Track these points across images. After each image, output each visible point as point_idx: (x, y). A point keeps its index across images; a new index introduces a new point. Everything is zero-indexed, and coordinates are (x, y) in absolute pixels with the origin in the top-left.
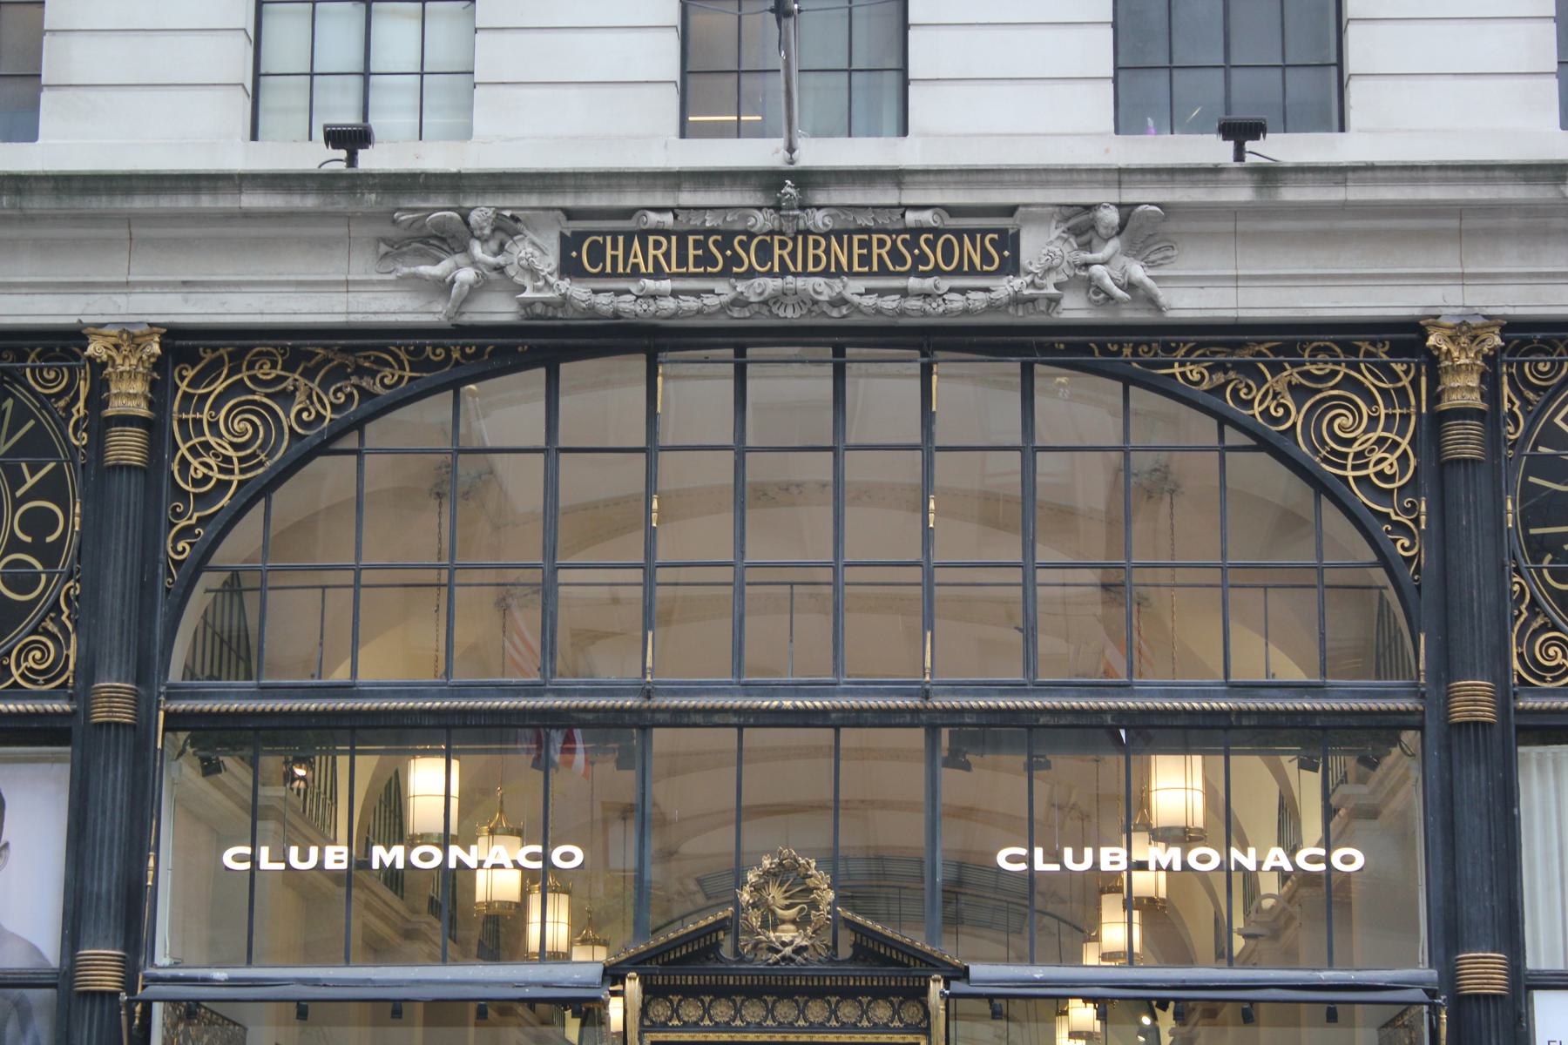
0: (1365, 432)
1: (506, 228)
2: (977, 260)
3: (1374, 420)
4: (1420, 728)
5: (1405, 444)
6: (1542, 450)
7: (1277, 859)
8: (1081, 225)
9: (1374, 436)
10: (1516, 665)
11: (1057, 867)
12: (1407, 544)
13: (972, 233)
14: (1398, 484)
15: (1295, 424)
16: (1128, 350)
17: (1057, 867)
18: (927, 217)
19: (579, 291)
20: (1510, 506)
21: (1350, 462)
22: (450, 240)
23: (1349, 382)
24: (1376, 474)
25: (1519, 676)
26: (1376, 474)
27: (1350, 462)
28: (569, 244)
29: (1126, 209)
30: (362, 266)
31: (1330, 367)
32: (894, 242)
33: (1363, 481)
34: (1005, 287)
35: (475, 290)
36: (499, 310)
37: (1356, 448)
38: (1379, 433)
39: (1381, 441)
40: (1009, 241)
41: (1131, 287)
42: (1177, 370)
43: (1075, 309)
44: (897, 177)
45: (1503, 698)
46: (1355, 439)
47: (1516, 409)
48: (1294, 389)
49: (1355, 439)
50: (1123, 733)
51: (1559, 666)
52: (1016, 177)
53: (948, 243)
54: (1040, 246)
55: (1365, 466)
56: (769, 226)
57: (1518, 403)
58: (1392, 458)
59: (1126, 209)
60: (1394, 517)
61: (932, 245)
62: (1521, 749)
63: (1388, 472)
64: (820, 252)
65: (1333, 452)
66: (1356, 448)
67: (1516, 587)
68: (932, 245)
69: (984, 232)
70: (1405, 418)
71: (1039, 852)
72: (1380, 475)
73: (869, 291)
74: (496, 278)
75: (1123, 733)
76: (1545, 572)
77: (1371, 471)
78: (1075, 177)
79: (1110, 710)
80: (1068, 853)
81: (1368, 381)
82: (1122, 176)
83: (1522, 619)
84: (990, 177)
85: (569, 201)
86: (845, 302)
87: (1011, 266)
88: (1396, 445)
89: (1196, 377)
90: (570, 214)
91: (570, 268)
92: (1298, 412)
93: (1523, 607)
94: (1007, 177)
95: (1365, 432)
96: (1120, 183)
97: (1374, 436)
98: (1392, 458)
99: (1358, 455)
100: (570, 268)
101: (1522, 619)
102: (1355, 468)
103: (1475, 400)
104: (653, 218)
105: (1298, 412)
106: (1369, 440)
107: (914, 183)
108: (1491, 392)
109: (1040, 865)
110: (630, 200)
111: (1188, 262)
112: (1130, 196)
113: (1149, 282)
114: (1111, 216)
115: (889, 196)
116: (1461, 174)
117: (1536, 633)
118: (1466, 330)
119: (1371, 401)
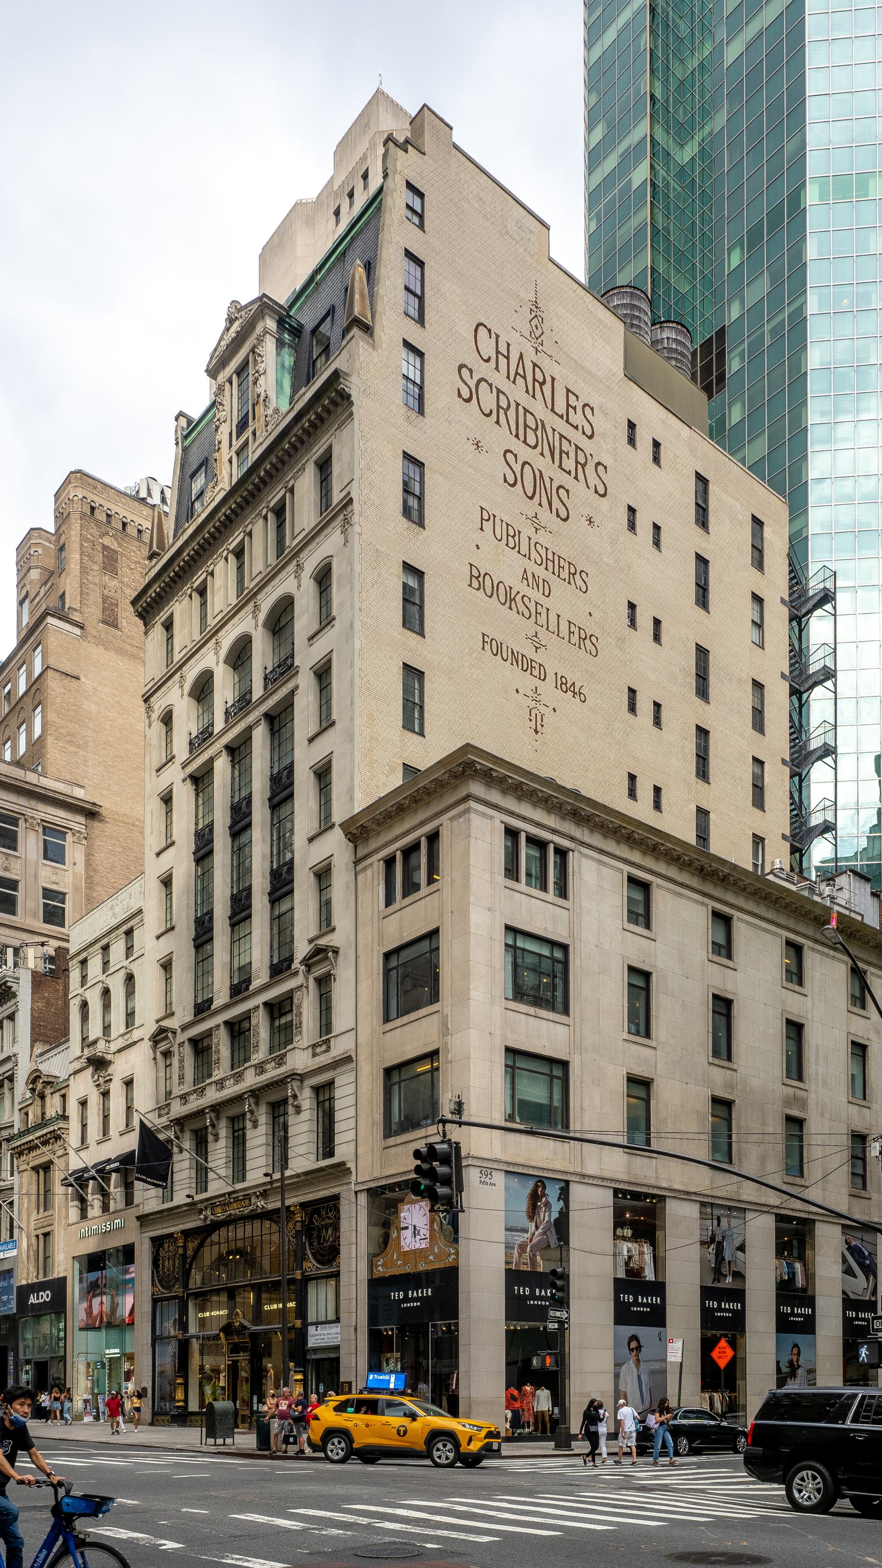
1: (206, 1208)
22: (200, 1212)
36: (208, 1222)
40: (250, 1200)
43: (259, 1211)
54: (253, 1201)
103: (299, 1219)
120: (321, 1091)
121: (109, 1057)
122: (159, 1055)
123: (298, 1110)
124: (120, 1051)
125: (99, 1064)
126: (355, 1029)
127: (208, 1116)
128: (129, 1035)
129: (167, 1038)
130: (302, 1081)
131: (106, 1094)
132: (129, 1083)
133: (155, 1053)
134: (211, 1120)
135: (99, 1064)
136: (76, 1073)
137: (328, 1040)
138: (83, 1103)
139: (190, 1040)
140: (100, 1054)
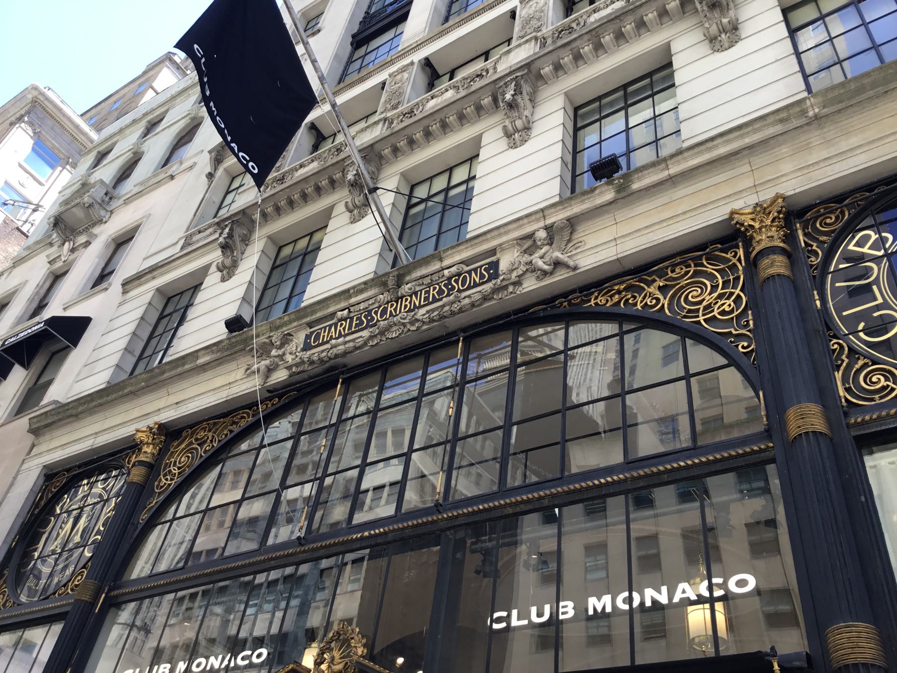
0: (710, 294)
2: (477, 280)
3: (714, 288)
4: (773, 461)
5: (737, 291)
6: (841, 266)
7: (684, 592)
8: (528, 243)
9: (715, 295)
10: (842, 392)
11: (525, 622)
12: (746, 344)
13: (475, 270)
14: (736, 313)
15: (663, 305)
16: (568, 305)
17: (525, 622)
18: (454, 270)
20: (817, 297)
21: (700, 314)
23: (696, 274)
24: (719, 313)
25: (847, 400)
26: (719, 313)
27: (700, 314)
29: (547, 228)
31: (685, 270)
32: (440, 287)
33: (711, 320)
37: (705, 303)
38: (719, 291)
39: (720, 297)
42: (592, 302)
46: (704, 300)
47: (814, 248)
48: (660, 288)
49: (704, 300)
50: (557, 510)
51: (884, 388)
52: (493, 234)
53: (465, 277)
55: (713, 311)
56: (386, 300)
57: (815, 244)
58: (730, 301)
59: (547, 228)
60: (734, 332)
61: (457, 281)
62: (870, 461)
63: (727, 309)
64: (407, 303)
65: (689, 311)
66: (705, 303)
67: (836, 346)
68: (457, 281)
69: (481, 267)
70: (738, 278)
71: (515, 613)
72: (723, 313)
73: (428, 312)
75: (557, 510)
76: (861, 334)
77: (715, 313)
78: (521, 222)
79: (546, 495)
80: (534, 610)
81: (710, 269)
83: (844, 364)
84: (481, 239)
85: (308, 319)
86: (417, 320)
88: (732, 294)
89: (604, 302)
90: (310, 325)
92: (665, 298)
93: (844, 357)
94: (489, 236)
95: (710, 294)
96: (544, 217)
97: (715, 295)
98: (730, 301)
99: (705, 308)
101: (844, 364)
102: (703, 315)
104: (339, 313)
105: (665, 298)
106: (712, 297)
107: (447, 256)
108: (790, 238)
109: (515, 622)
110: (332, 309)
112: (549, 221)
113: (566, 259)
114: (542, 234)
116: (737, 133)
117: (859, 371)
118: (760, 209)
119: (711, 277)
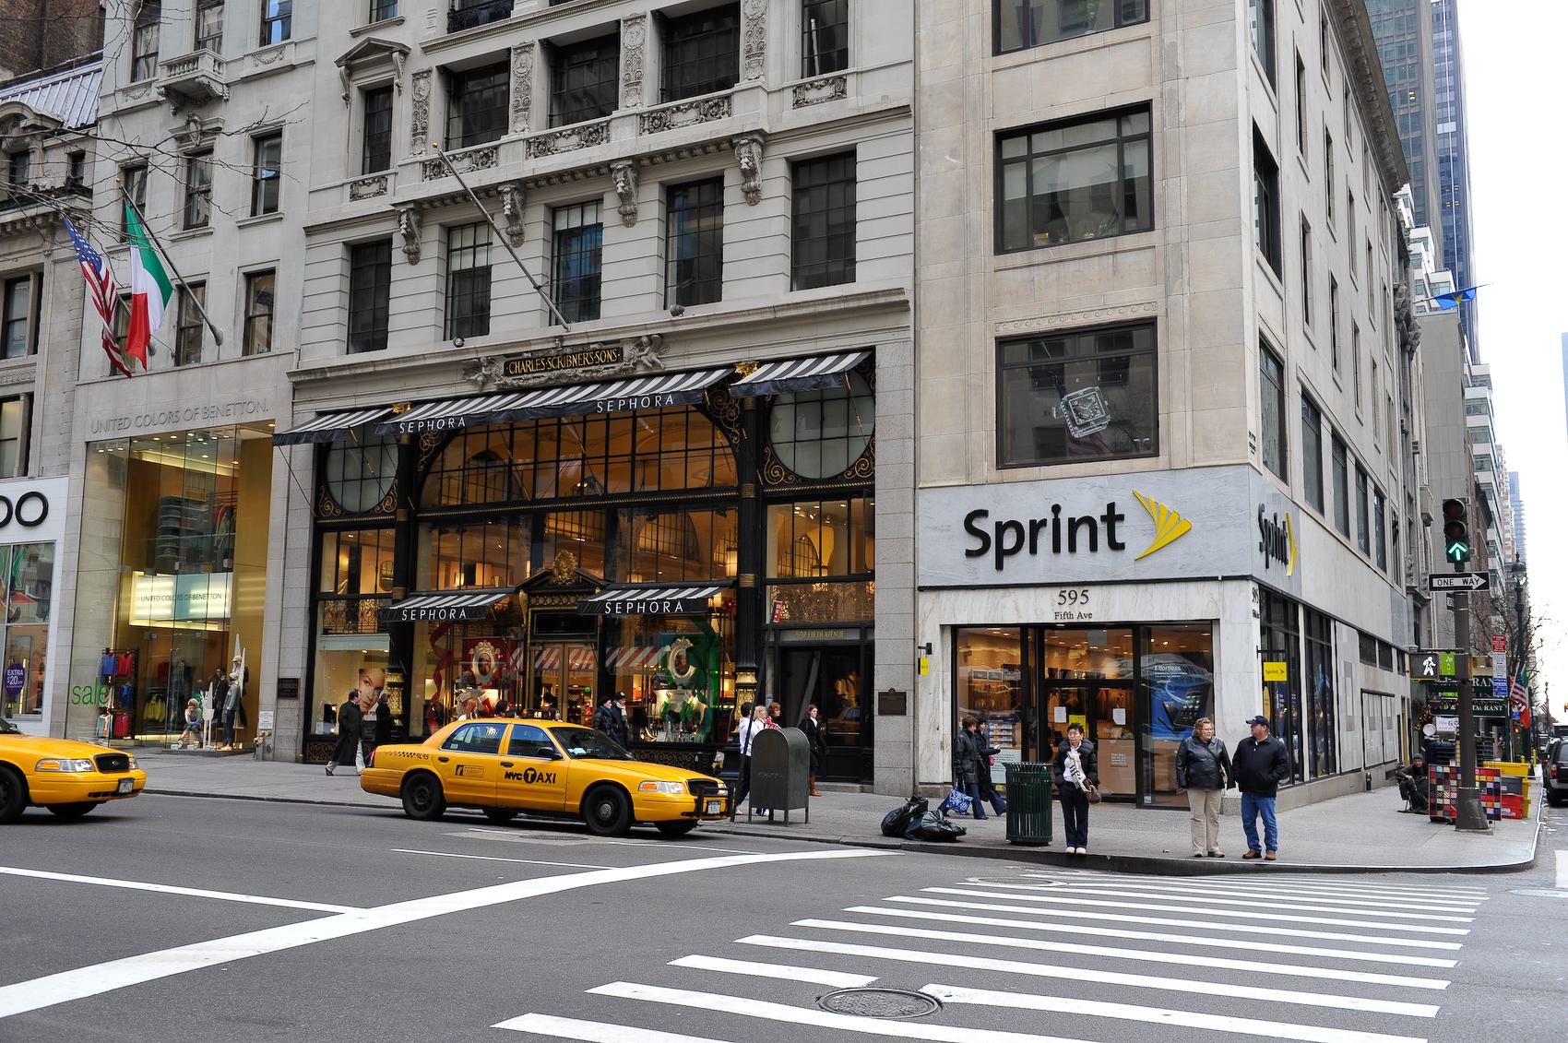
19: (509, 380)
28: (506, 365)
30: (458, 378)
34: (618, 366)
35: (484, 384)
40: (620, 351)
41: (653, 363)
44: (586, 335)
45: (758, 489)
54: (628, 351)
74: (488, 378)
82: (645, 327)
87: (619, 360)
91: (507, 374)
100: (507, 374)
111: (674, 351)
115: (585, 341)
120: (802, 170)
121: (218, 89)
122: (355, 94)
123: (752, 196)
124: (247, 80)
125: (190, 99)
126: (914, 62)
127: (507, 198)
128: (274, 55)
129: (389, 59)
130: (763, 147)
131: (196, 157)
132: (266, 141)
133: (346, 87)
134: (514, 206)
135: (190, 99)
136: (117, 115)
137: (842, 79)
138: (133, 171)
139: (444, 71)
140: (205, 81)
